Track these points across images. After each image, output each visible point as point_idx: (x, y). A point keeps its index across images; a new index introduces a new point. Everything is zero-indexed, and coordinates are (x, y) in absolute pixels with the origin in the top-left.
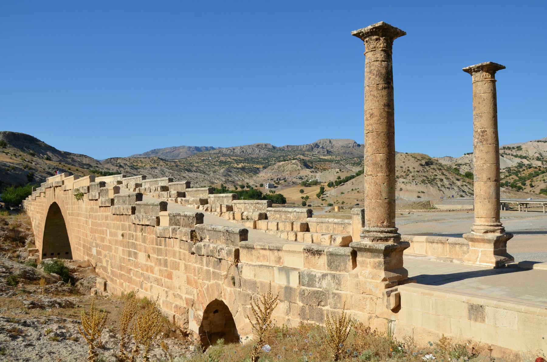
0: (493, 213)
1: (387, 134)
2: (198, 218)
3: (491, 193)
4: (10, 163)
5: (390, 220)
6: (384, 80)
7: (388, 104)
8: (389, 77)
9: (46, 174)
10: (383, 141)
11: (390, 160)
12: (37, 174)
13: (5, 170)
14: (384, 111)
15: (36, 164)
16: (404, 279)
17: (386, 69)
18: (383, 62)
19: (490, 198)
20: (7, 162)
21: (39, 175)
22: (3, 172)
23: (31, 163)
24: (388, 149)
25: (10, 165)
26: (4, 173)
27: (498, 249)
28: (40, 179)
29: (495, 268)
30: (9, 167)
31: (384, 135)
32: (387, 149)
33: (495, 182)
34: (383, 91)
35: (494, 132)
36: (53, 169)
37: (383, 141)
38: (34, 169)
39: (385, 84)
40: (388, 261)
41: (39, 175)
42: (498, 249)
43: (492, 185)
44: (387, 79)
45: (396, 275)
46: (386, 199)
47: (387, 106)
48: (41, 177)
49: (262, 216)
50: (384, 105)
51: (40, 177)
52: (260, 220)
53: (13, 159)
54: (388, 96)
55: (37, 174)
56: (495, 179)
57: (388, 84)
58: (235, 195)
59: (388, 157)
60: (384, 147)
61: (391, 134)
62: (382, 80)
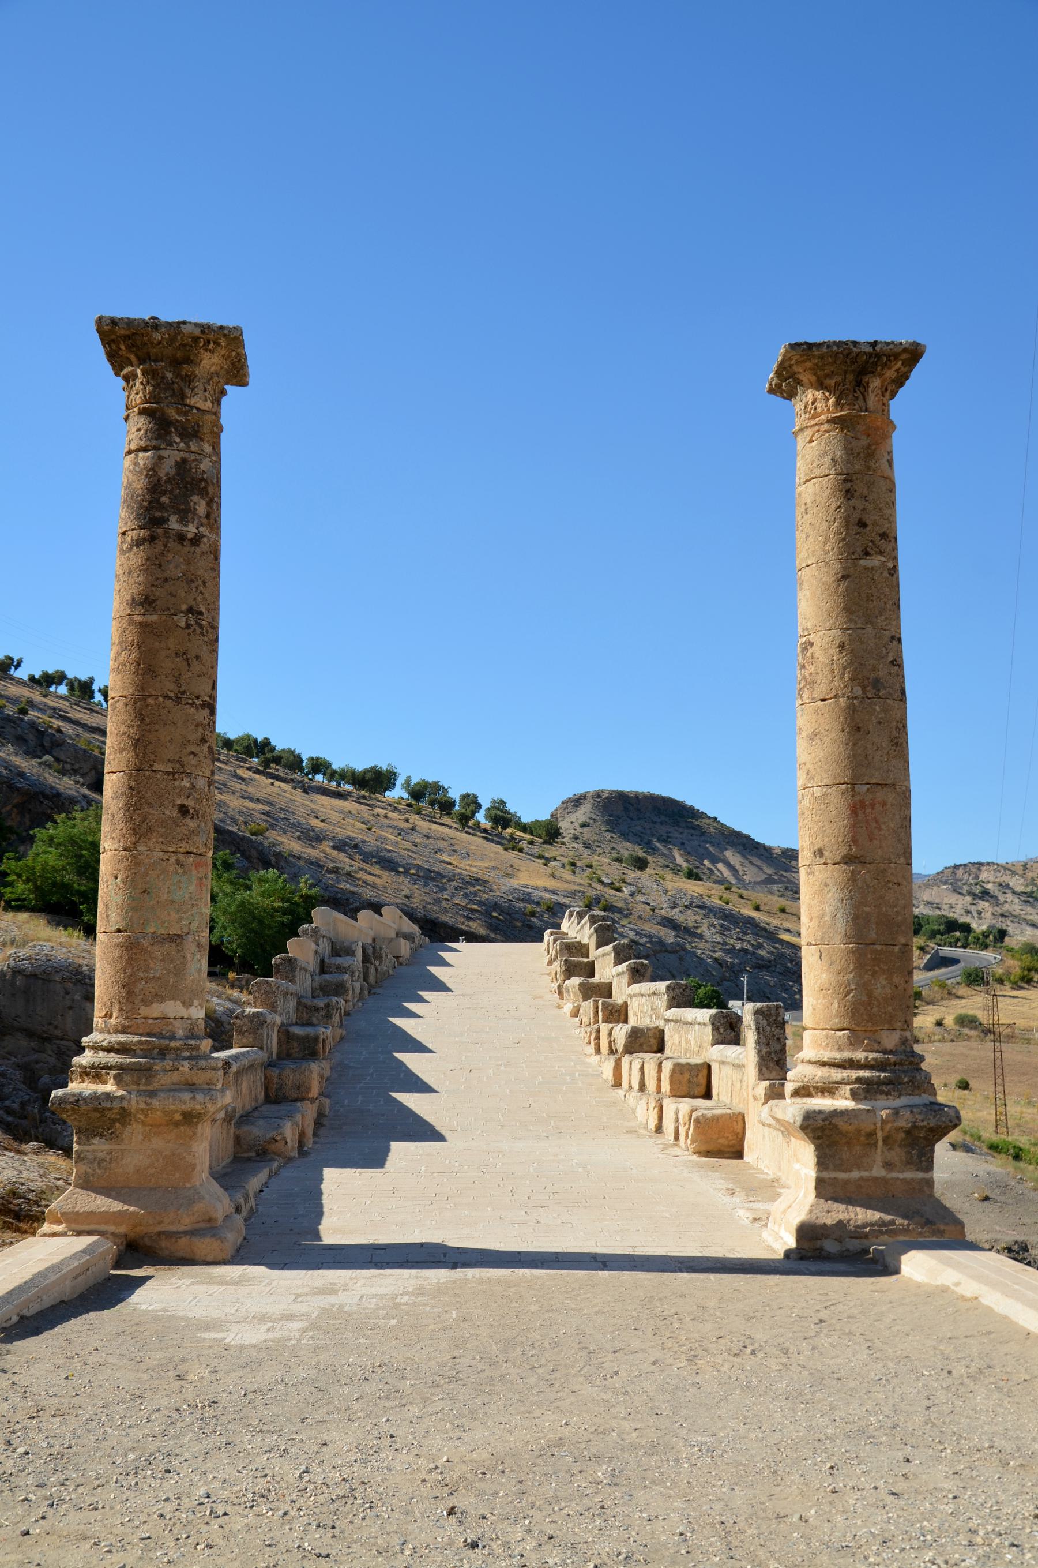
0: (836, 1005)
1: (135, 703)
2: (245, 1028)
3: (827, 918)
4: (546, 890)
5: (130, 1006)
6: (138, 517)
7: (147, 598)
8: (158, 501)
9: (658, 923)
10: (123, 728)
11: (139, 792)
12: (624, 926)
13: (525, 914)
14: (131, 622)
15: (632, 895)
16: (159, 1228)
17: (147, 475)
18: (141, 454)
19: (822, 938)
20: (537, 888)
21: (631, 929)
22: (517, 920)
23: (619, 890)
24: (137, 756)
25: (541, 898)
26: (519, 924)
27: (855, 1174)
28: (632, 941)
29: (788, 1254)
30: (538, 903)
31: (126, 705)
32: (132, 754)
33: (843, 867)
34: (131, 555)
35: (842, 646)
36: (686, 907)
37: (123, 728)
38: (620, 911)
39: (140, 528)
40: (100, 1155)
41: (631, 929)
42: (855, 1174)
43: (830, 882)
44: (147, 509)
45: (117, 1206)
46: (119, 931)
47: (141, 604)
48: (638, 933)
49: (642, 1040)
50: (133, 603)
51: (632, 935)
52: (631, 1053)
53: (559, 879)
54: (146, 570)
55: (624, 926)
56: (844, 850)
57: (150, 529)
58: (642, 964)
59: (133, 784)
60: (124, 749)
61: (151, 701)
62: (132, 517)
